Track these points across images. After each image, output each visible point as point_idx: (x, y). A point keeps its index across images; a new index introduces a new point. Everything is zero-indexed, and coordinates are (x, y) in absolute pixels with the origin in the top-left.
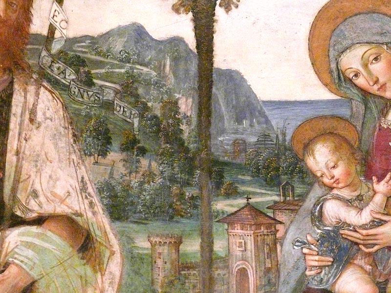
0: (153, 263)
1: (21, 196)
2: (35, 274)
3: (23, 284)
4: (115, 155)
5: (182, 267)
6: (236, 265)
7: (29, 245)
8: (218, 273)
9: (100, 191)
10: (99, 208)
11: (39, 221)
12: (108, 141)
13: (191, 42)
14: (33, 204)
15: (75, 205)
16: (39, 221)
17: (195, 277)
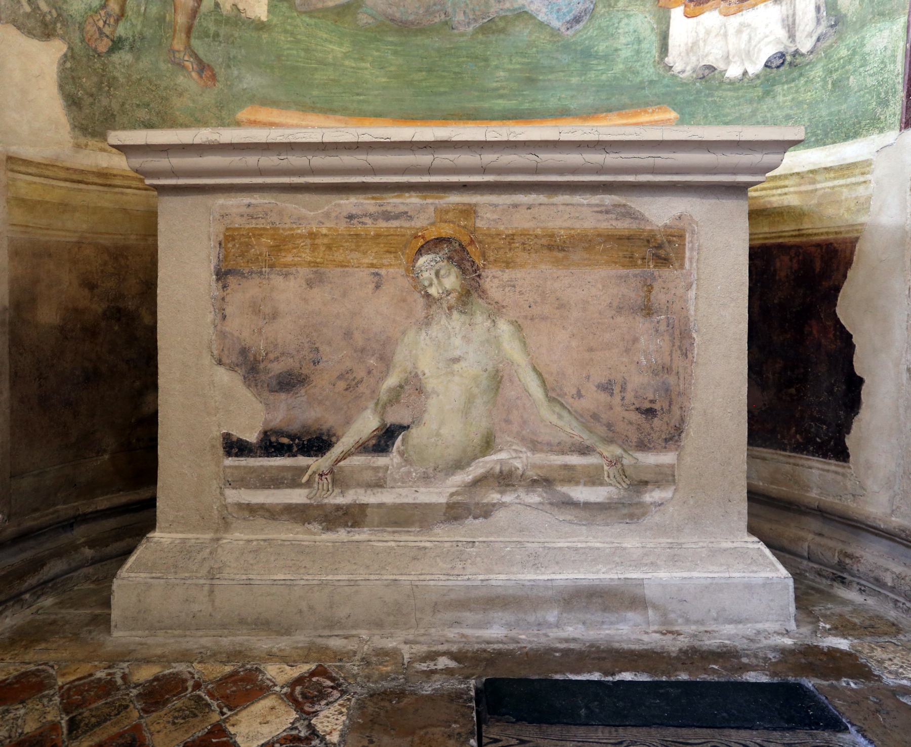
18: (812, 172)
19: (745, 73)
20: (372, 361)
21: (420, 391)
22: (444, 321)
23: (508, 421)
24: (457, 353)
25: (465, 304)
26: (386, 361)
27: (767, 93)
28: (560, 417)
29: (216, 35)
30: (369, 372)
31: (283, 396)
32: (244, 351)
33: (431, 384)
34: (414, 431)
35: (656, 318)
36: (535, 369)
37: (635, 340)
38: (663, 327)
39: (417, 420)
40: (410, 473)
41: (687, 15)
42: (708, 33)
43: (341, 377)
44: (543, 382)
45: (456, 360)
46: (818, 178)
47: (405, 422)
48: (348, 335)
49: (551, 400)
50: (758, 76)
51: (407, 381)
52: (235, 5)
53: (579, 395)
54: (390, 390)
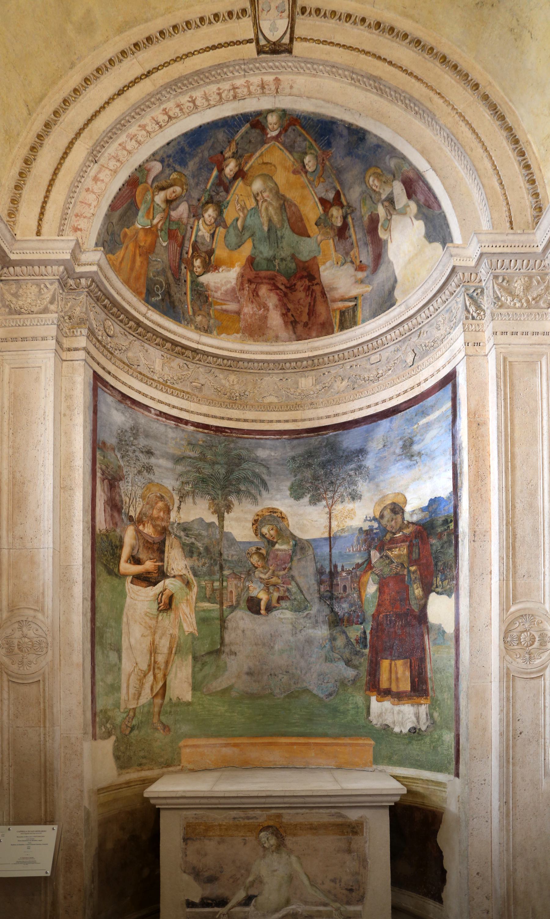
0: (206, 589)
1: (169, 570)
2: (173, 592)
3: (170, 594)
4: (195, 557)
5: (213, 590)
6: (229, 589)
7: (172, 584)
8: (225, 592)
9: (191, 568)
10: (191, 573)
11: (174, 577)
12: (193, 553)
13: (217, 523)
14: (172, 572)
15: (184, 572)
16: (174, 577)
17: (218, 593)
18: (427, 780)
19: (401, 731)
20: (243, 871)
21: (261, 882)
22: (270, 856)
23: (295, 894)
24: (276, 868)
25: (278, 850)
26: (248, 871)
27: (410, 742)
28: (316, 892)
29: (170, 712)
30: (242, 876)
31: (209, 885)
32: (194, 868)
33: (266, 880)
34: (259, 898)
35: (353, 854)
36: (306, 874)
37: (345, 863)
38: (356, 857)
39: (260, 894)
40: (257, 914)
41: (378, 701)
42: (386, 710)
43: (231, 877)
44: (309, 879)
45: (275, 871)
46: (430, 784)
47: (256, 894)
48: (234, 862)
49: (312, 885)
50: (406, 734)
51: (256, 879)
52: (178, 698)
53: (323, 883)
54: (250, 882)
